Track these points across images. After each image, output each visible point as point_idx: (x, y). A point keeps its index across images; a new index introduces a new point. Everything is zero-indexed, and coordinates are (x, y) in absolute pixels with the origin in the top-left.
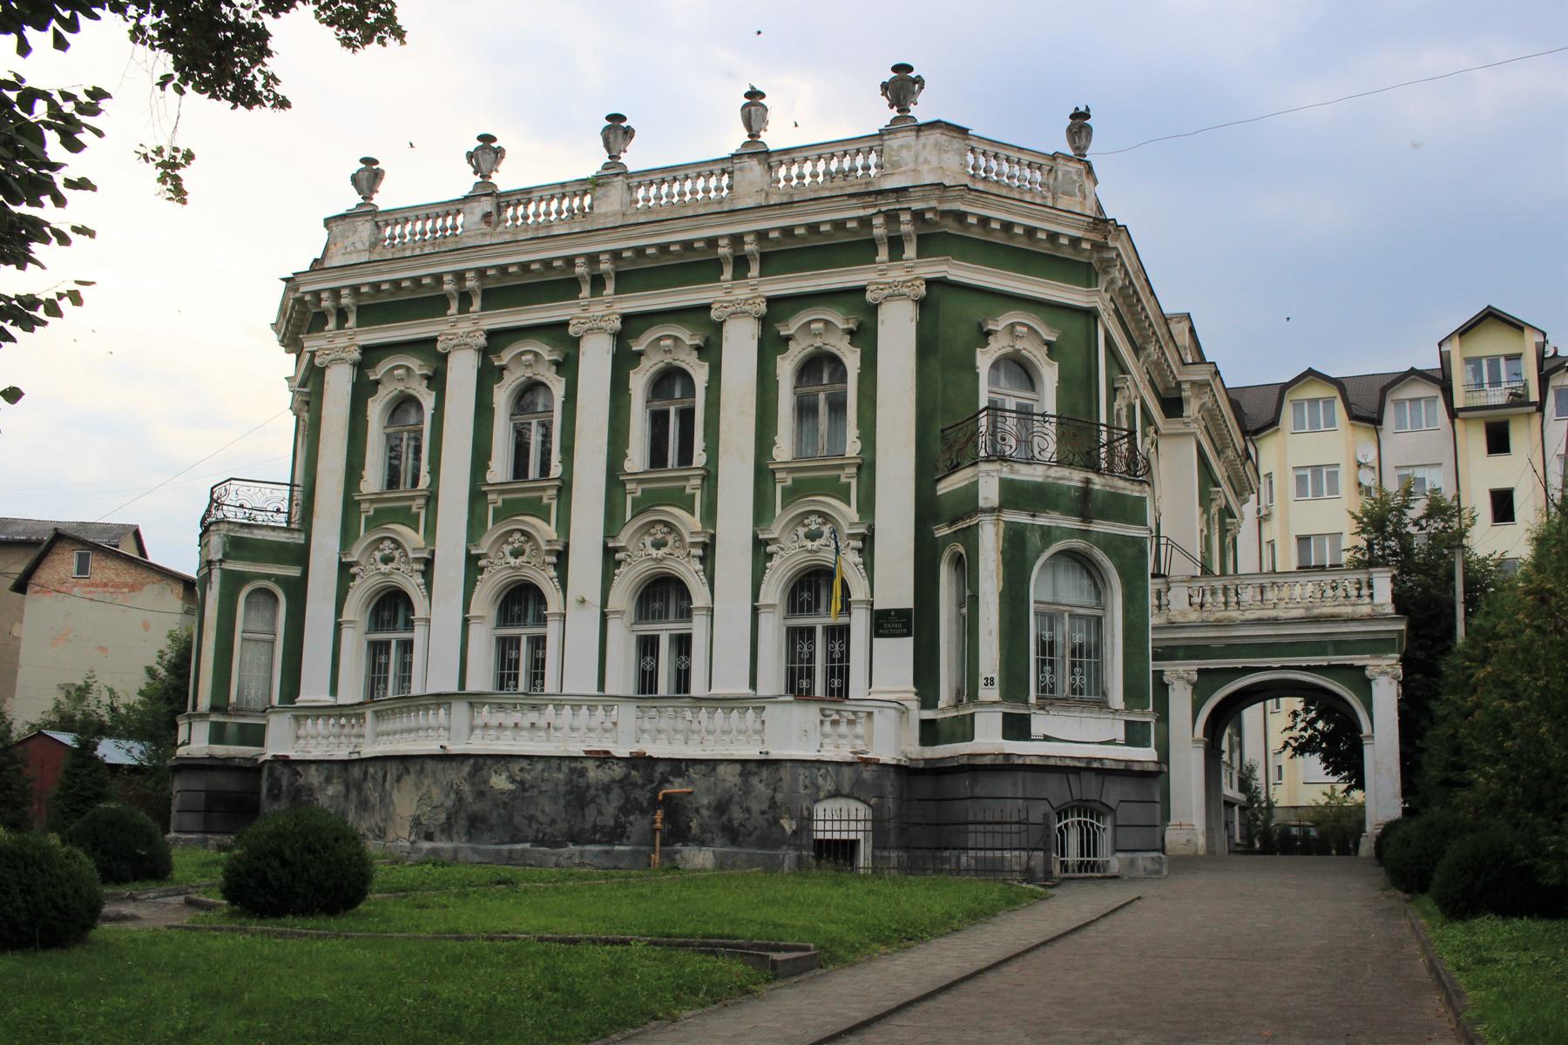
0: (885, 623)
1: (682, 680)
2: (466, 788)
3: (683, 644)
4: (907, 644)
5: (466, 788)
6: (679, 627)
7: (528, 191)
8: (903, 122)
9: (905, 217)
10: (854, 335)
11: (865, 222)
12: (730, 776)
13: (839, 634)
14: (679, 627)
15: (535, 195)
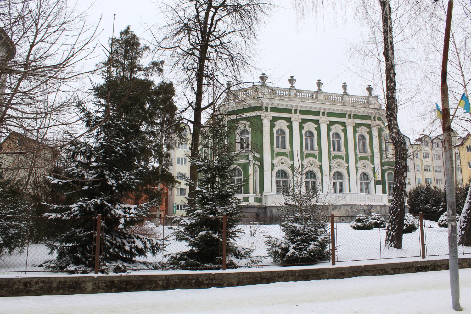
0: (377, 183)
1: (341, 191)
2: (350, 211)
3: (341, 184)
4: (381, 186)
5: (350, 211)
6: (341, 181)
7: (303, 91)
8: (370, 95)
9: (377, 113)
10: (368, 133)
11: (371, 113)
12: (378, 208)
13: (367, 184)
14: (341, 181)
15: (305, 92)
